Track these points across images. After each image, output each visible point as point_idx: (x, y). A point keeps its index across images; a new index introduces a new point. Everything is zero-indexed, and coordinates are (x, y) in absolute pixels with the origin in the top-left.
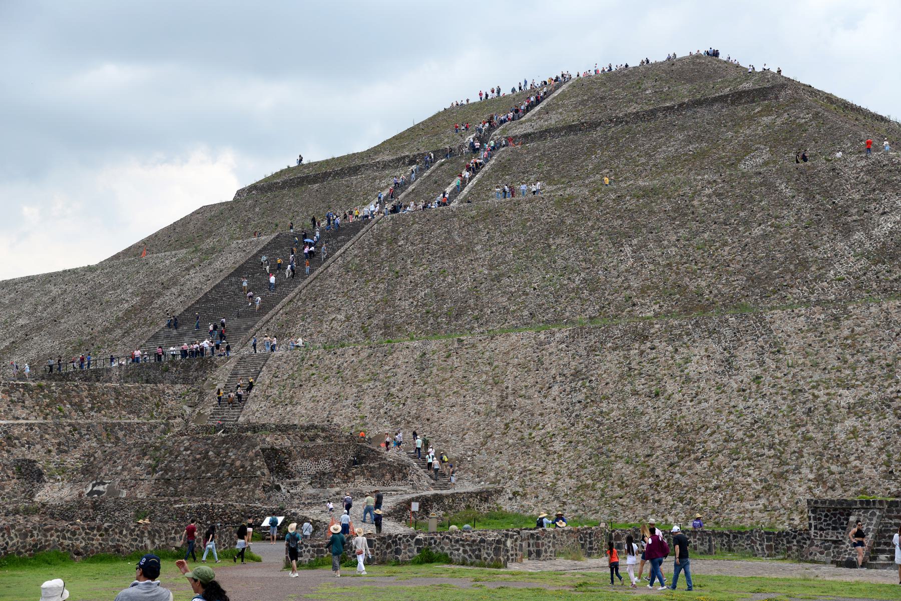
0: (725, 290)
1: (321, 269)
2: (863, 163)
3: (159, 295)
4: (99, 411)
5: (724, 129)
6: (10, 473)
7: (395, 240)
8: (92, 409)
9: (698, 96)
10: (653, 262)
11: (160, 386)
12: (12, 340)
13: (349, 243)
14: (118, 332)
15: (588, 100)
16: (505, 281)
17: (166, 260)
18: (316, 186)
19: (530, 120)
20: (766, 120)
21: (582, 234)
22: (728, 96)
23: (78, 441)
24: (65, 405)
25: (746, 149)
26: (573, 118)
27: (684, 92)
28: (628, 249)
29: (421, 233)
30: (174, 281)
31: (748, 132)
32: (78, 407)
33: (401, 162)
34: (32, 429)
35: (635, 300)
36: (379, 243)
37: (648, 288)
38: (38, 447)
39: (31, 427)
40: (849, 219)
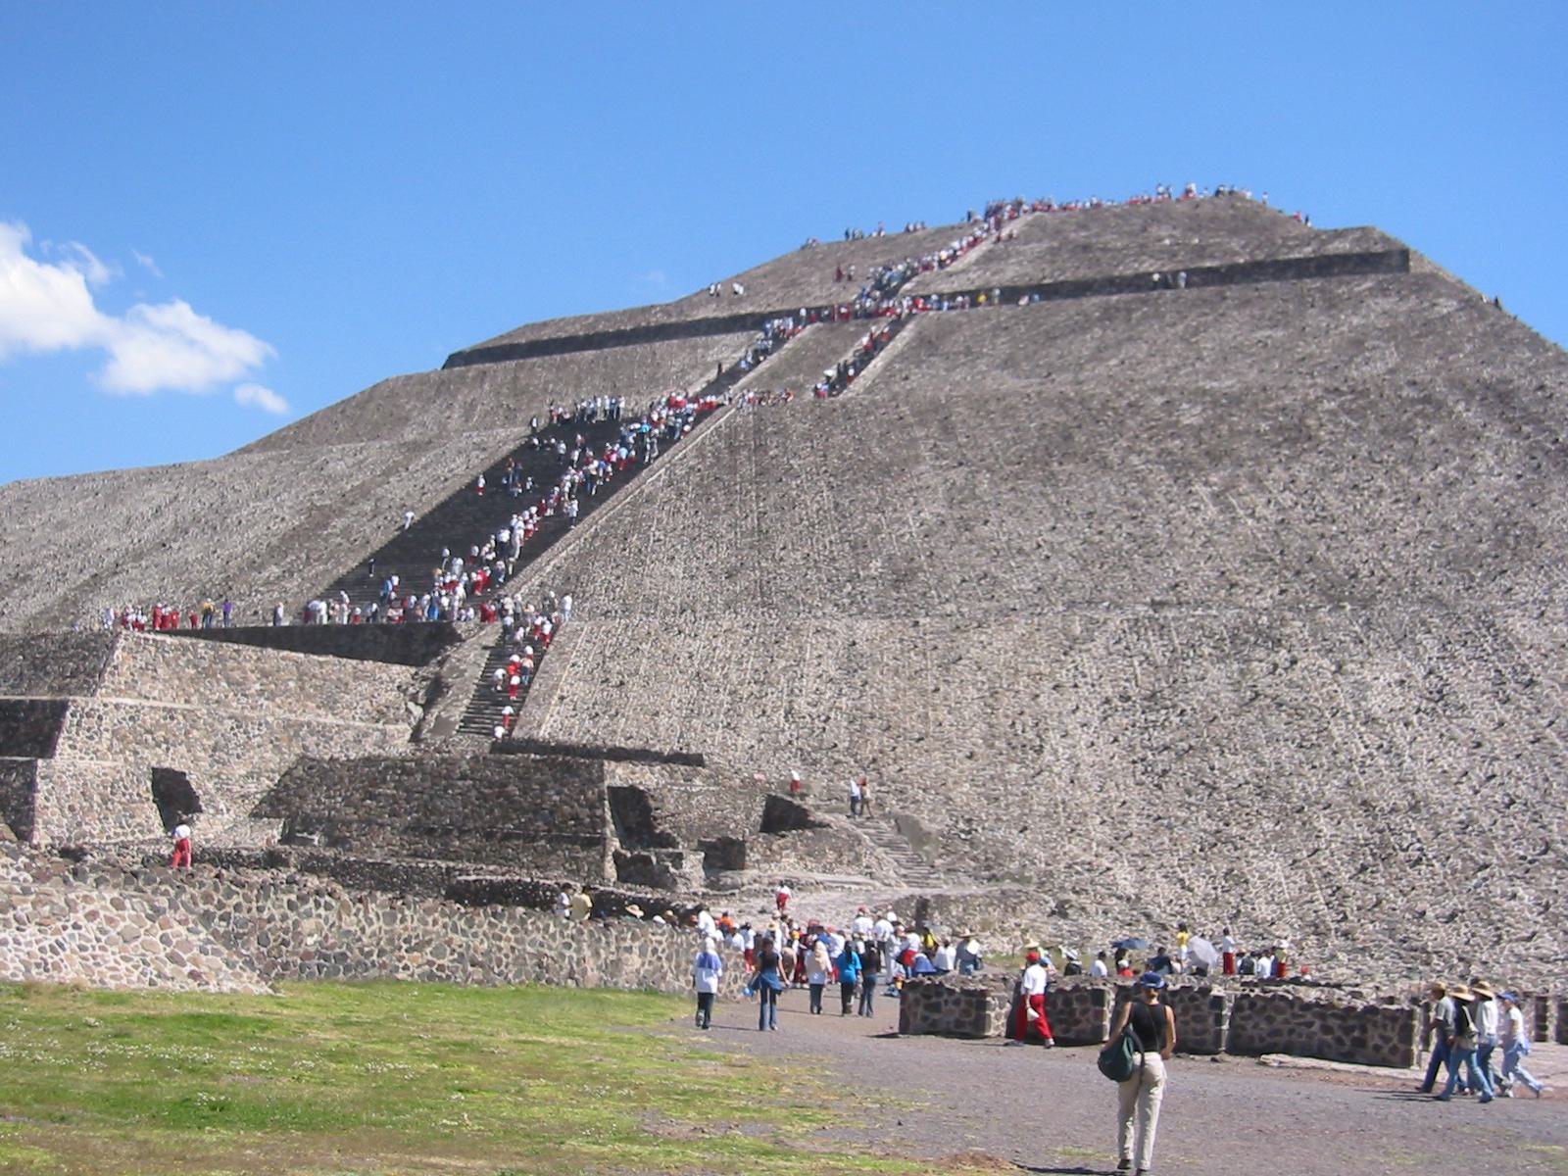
0: (1397, 572)
4: (271, 698)
7: (761, 448)
9: (1260, 256)
11: (369, 664)
15: (1059, 249)
20: (1385, 303)
22: (1308, 260)
24: (218, 681)
27: (1240, 251)
29: (807, 437)
30: (364, 492)
31: (1356, 321)
34: (172, 718)
38: (183, 749)
39: (171, 713)
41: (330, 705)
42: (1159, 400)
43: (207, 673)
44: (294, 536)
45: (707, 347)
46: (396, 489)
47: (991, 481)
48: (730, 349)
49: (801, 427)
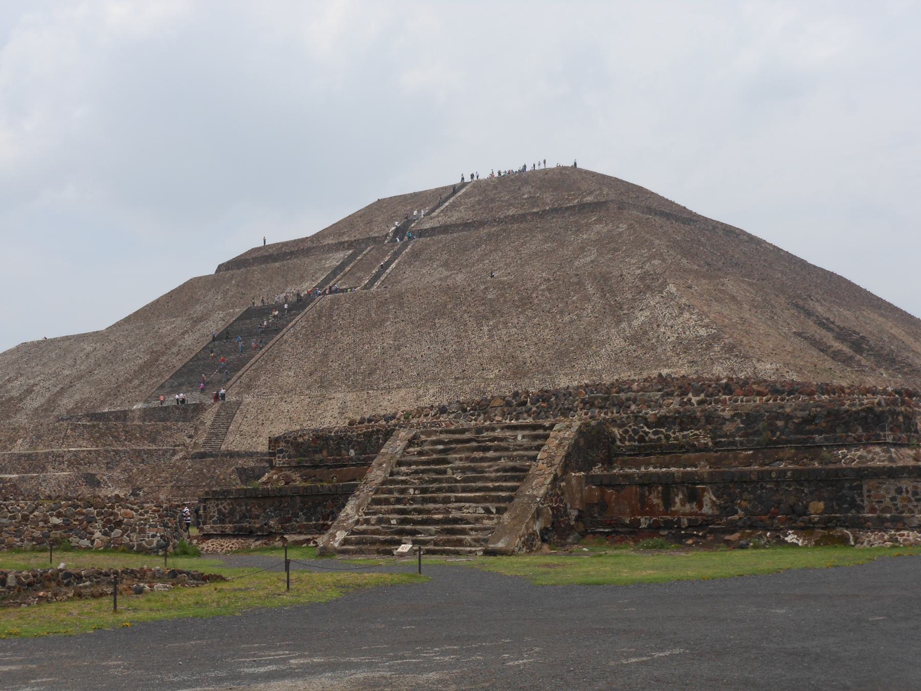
0: (540, 361)
1: (278, 337)
2: (639, 271)
3: (163, 354)
5: (570, 233)
6: (80, 481)
8: (125, 440)
10: (500, 339)
11: (169, 424)
12: (61, 386)
13: (299, 317)
14: (136, 382)
16: (404, 350)
17: (166, 327)
18: (277, 264)
19: (438, 216)
20: (598, 227)
21: (458, 315)
22: (575, 206)
23: (119, 461)
25: (582, 249)
26: (468, 216)
28: (485, 328)
29: (349, 310)
30: (173, 343)
31: (585, 237)
32: (116, 438)
33: (339, 246)
35: (485, 366)
36: (320, 317)
37: (494, 357)
38: (95, 465)
39: (90, 452)
40: (622, 313)
41: (154, 441)
42: (482, 287)
43: (102, 435)
44: (142, 369)
45: (326, 259)
46: (188, 340)
47: (412, 329)
48: (338, 257)
49: (347, 305)
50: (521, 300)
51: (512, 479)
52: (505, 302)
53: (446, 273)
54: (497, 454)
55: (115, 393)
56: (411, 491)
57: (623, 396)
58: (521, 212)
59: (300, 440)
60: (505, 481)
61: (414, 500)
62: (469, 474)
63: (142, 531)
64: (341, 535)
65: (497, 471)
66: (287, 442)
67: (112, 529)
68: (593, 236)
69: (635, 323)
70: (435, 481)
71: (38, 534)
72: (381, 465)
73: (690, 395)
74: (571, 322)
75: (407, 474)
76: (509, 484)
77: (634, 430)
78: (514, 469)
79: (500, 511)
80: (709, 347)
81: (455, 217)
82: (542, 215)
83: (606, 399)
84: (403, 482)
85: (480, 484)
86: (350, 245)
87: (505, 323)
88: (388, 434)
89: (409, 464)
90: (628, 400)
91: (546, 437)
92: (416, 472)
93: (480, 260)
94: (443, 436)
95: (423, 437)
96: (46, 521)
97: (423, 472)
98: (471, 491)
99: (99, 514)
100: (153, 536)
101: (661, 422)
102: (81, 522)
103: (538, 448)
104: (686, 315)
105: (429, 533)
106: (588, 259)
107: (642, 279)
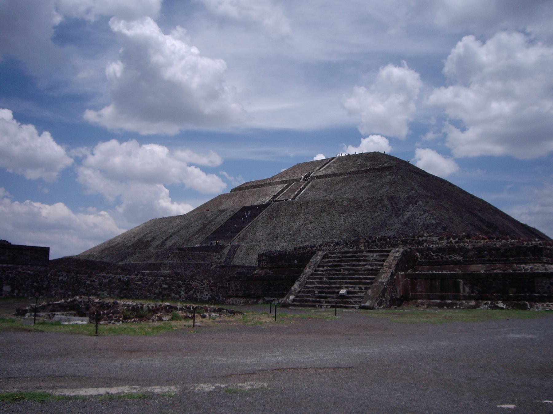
3: (208, 224)
7: (278, 211)
14: (197, 236)
20: (389, 177)
29: (285, 208)
30: (212, 220)
33: (281, 182)
36: (273, 211)
39: (178, 263)
41: (203, 260)
44: (199, 231)
46: (218, 220)
50: (358, 206)
51: (371, 274)
52: (351, 206)
53: (325, 194)
54: (365, 263)
55: (188, 240)
56: (325, 279)
57: (421, 239)
58: (357, 170)
59: (272, 255)
60: (368, 275)
61: (326, 283)
62: (351, 272)
63: (202, 292)
64: (292, 297)
65: (365, 271)
66: (266, 256)
67: (189, 291)
68: (387, 181)
69: (405, 217)
70: (336, 274)
71: (157, 291)
72: (310, 266)
73: (451, 239)
74: (379, 216)
75: (322, 271)
76: (370, 277)
77: (426, 254)
78: (372, 270)
79: (366, 289)
80: (436, 228)
81: (329, 171)
82: (366, 171)
83: (413, 240)
84: (320, 274)
85: (357, 276)
86: (286, 182)
87: (351, 215)
88: (313, 253)
89: (323, 267)
90: (423, 240)
91: (388, 256)
92: (326, 270)
93: (340, 189)
94: (339, 255)
95: (330, 255)
96: (161, 286)
97: (330, 270)
98: (352, 279)
99: (183, 284)
100: (207, 295)
101: (439, 250)
102: (176, 288)
103: (384, 261)
104: (427, 214)
105: (332, 298)
106: (385, 190)
107: (408, 198)
